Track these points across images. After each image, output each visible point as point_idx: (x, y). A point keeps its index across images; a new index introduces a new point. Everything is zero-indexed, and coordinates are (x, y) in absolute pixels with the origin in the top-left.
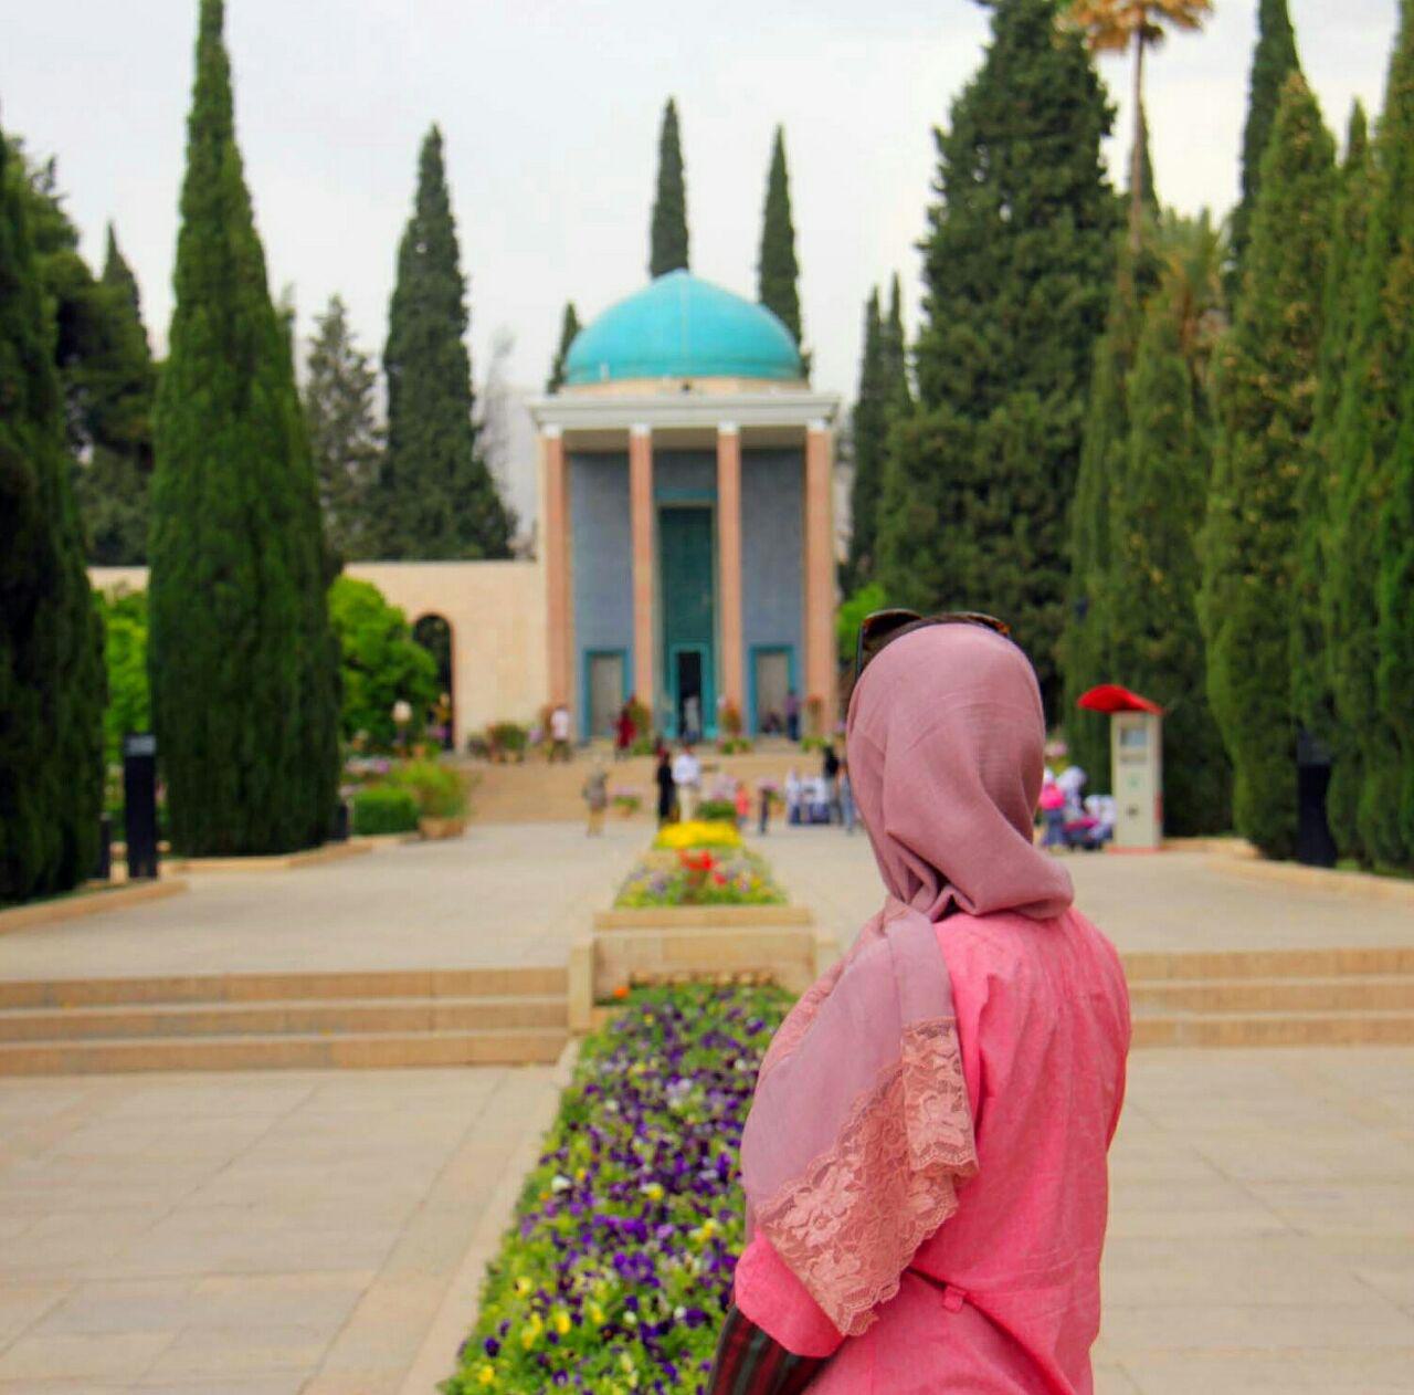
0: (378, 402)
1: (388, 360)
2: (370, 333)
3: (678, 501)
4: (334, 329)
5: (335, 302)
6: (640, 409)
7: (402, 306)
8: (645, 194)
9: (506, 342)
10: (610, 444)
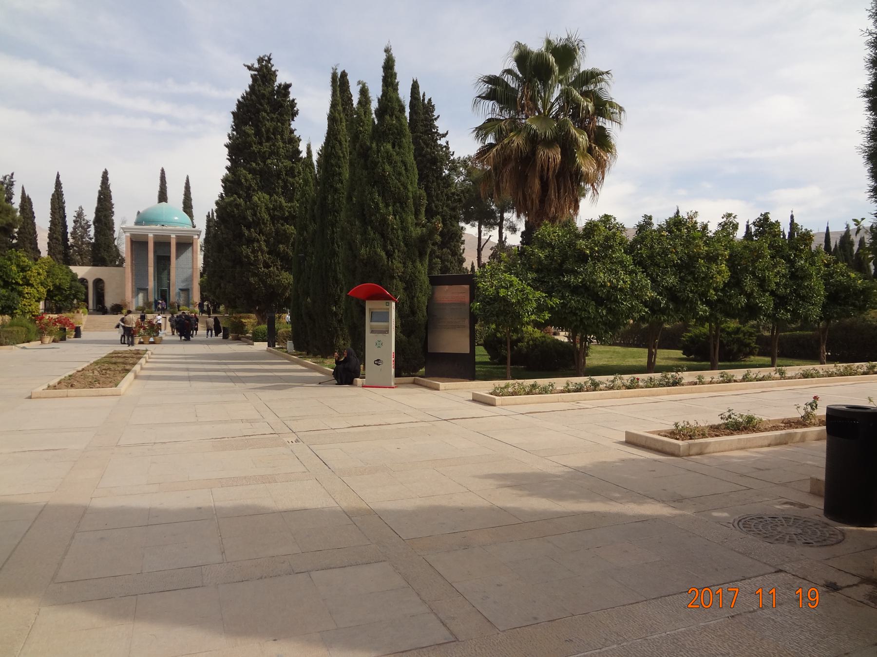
0: (92, 231)
1: (94, 223)
2: (90, 215)
3: (160, 251)
4: (80, 215)
5: (81, 208)
6: (151, 232)
7: (98, 211)
8: (157, 189)
9: (123, 220)
10: (142, 240)
